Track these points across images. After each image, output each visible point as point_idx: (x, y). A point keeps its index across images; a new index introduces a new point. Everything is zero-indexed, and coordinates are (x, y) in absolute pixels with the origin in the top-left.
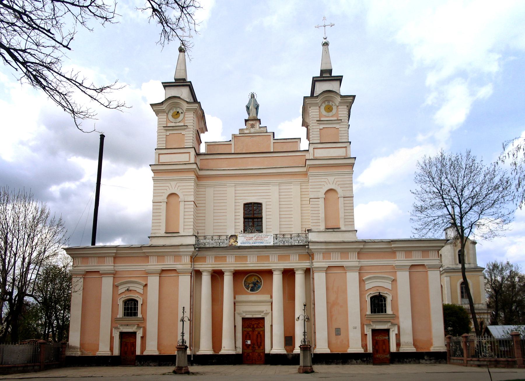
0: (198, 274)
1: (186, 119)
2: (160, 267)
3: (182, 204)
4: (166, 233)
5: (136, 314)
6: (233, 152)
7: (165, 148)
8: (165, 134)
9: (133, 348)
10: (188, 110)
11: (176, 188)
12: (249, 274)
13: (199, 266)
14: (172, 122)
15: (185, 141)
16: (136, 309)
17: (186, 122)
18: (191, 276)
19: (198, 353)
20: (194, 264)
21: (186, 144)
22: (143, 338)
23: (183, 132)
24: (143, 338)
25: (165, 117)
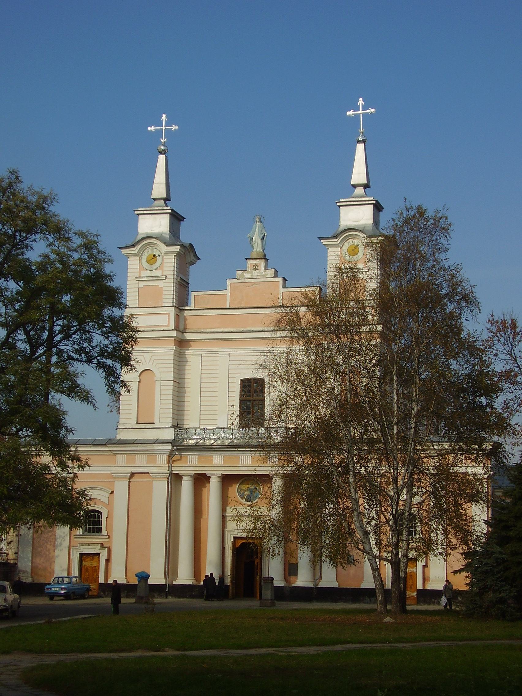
0: (176, 479)
1: (165, 265)
2: (129, 470)
3: (158, 384)
4: (138, 423)
5: (99, 530)
6: (228, 306)
7: (137, 306)
8: (137, 286)
9: (95, 574)
10: (166, 253)
11: (151, 363)
12: (244, 478)
13: (177, 469)
14: (147, 270)
15: (164, 297)
16: (99, 523)
17: (165, 269)
18: (168, 481)
19: (174, 583)
20: (171, 467)
21: (164, 301)
22: (108, 561)
23: (161, 284)
24: (108, 561)
25: (138, 262)
